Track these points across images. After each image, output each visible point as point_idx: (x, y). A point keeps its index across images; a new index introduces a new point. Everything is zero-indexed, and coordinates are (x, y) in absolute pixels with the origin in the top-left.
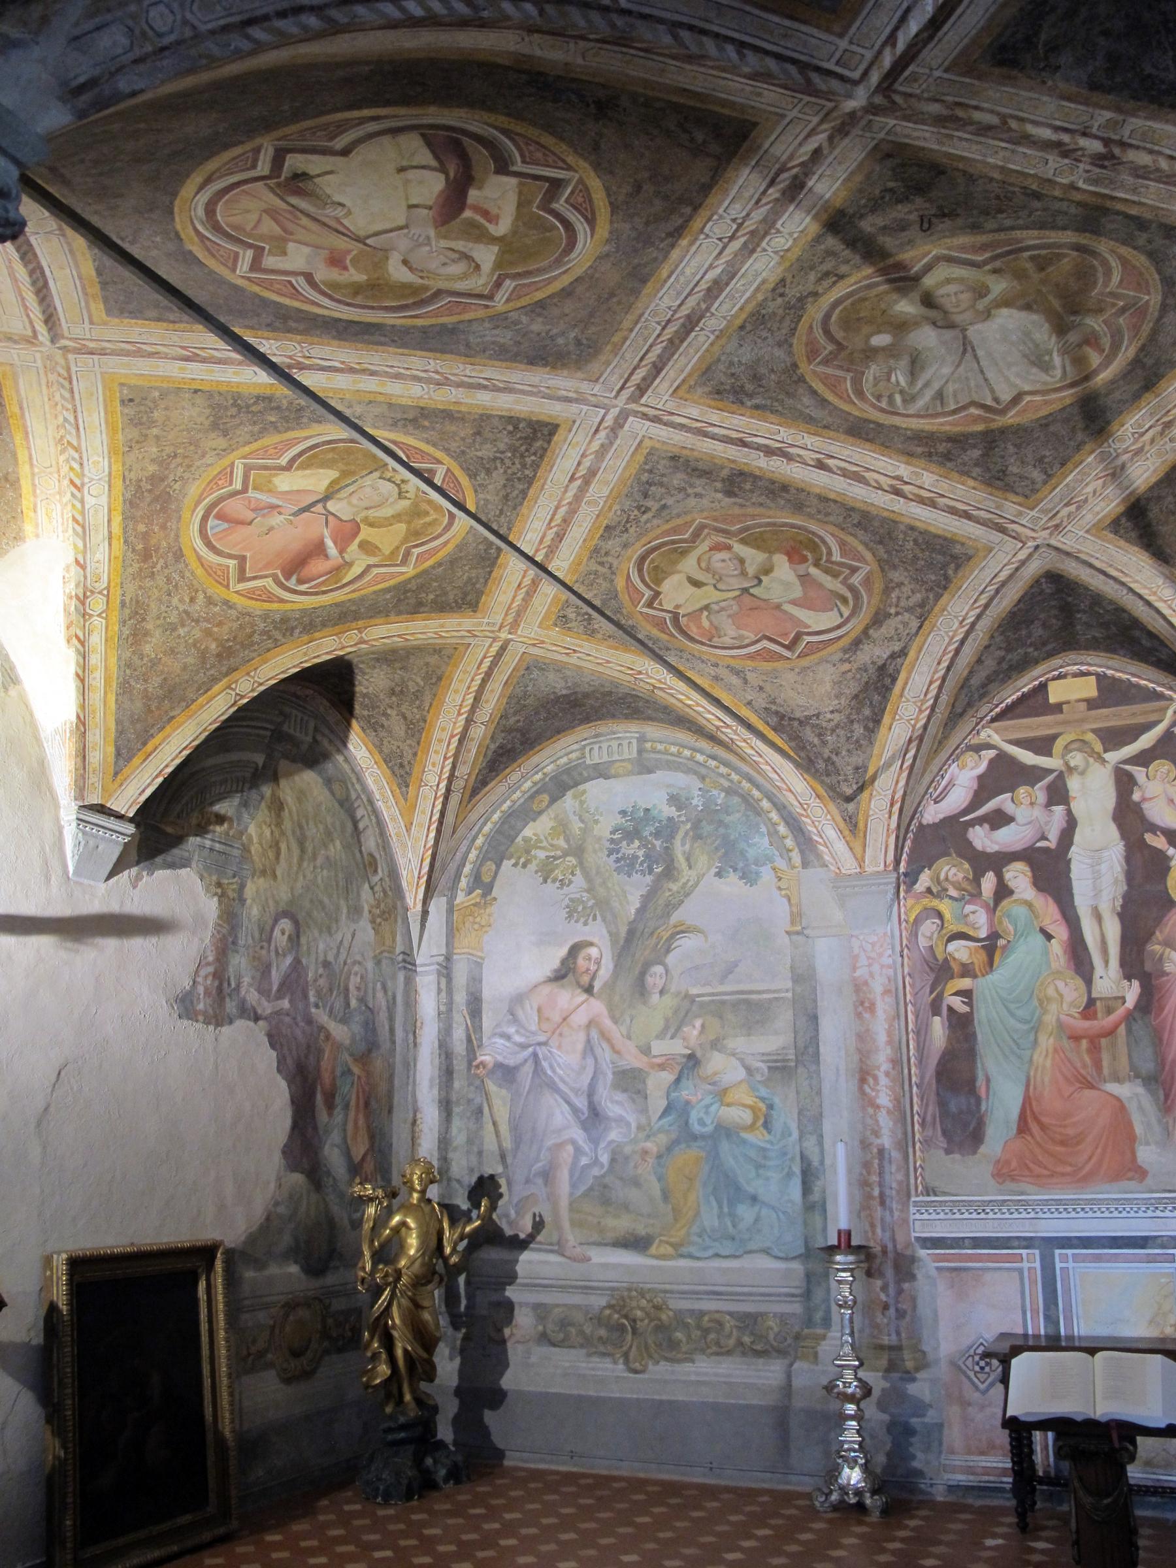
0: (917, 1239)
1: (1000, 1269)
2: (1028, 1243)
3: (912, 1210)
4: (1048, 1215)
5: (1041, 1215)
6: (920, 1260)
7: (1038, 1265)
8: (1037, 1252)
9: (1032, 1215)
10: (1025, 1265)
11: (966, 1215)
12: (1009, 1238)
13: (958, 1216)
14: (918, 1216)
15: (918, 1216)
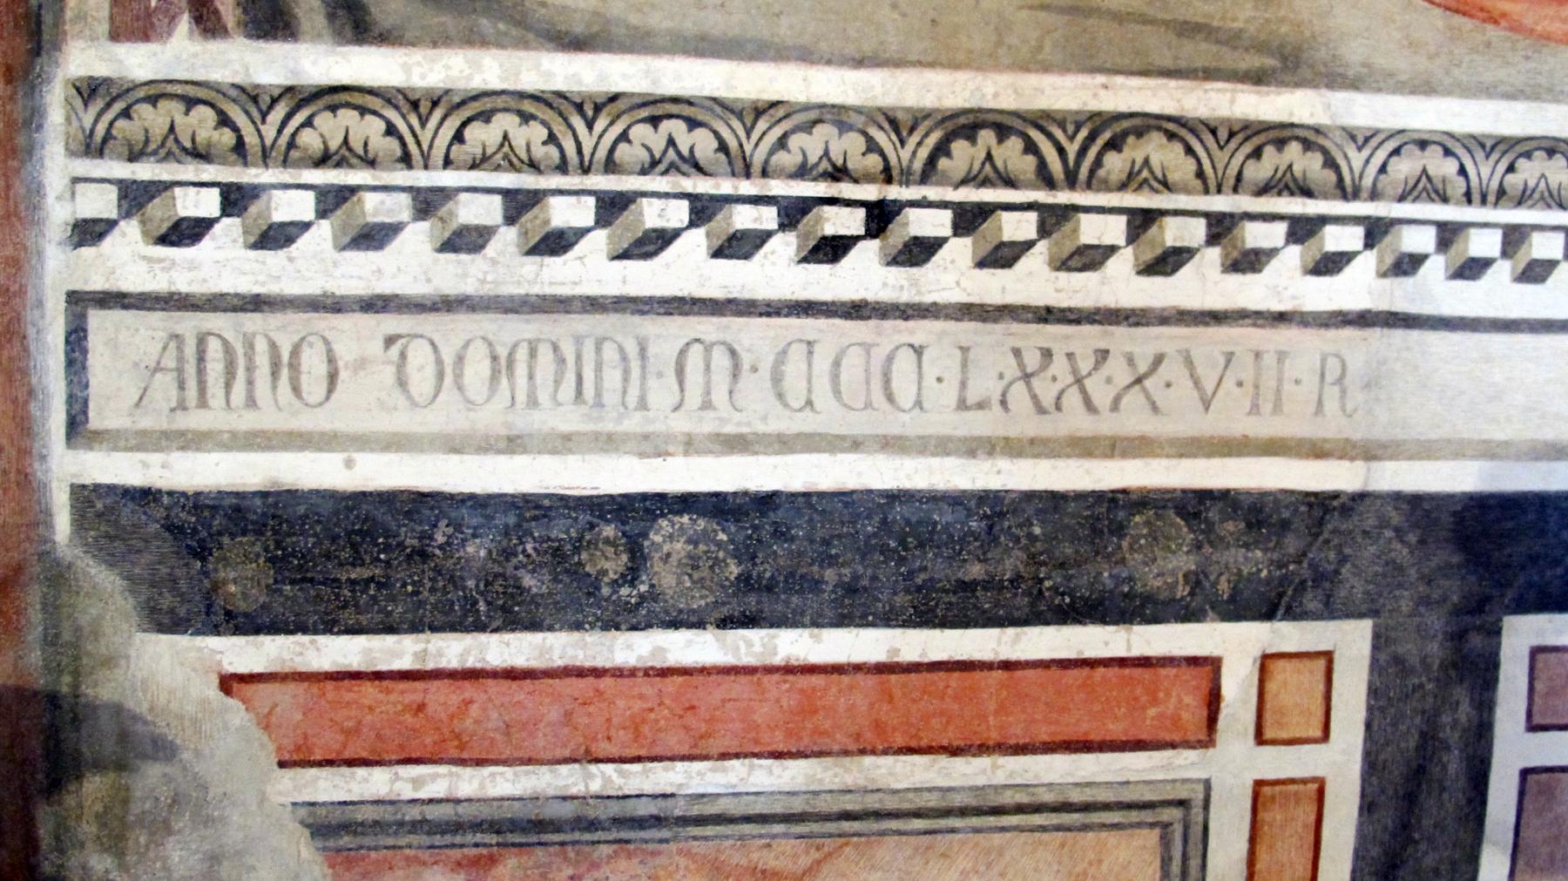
0: (94, 504)
1: (987, 809)
2: (1283, 552)
3: (68, 186)
4: (1497, 293)
5: (1432, 289)
6: (136, 742)
7: (1340, 762)
8: (1351, 641)
9: (1359, 286)
10: (1234, 764)
11: (689, 266)
12: (1110, 512)
13: (591, 268)
14: (128, 259)
15: (128, 259)
